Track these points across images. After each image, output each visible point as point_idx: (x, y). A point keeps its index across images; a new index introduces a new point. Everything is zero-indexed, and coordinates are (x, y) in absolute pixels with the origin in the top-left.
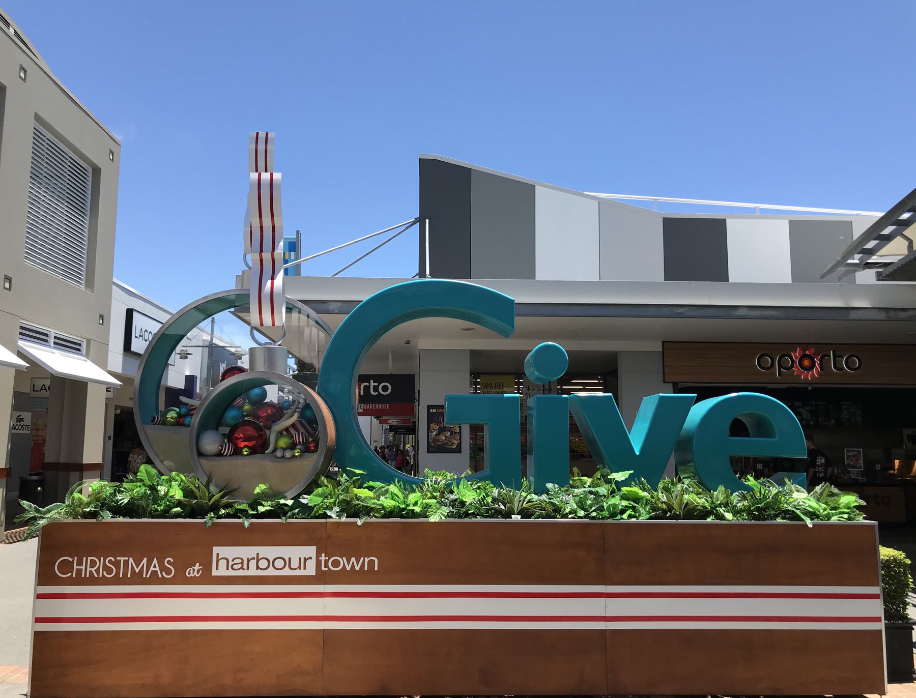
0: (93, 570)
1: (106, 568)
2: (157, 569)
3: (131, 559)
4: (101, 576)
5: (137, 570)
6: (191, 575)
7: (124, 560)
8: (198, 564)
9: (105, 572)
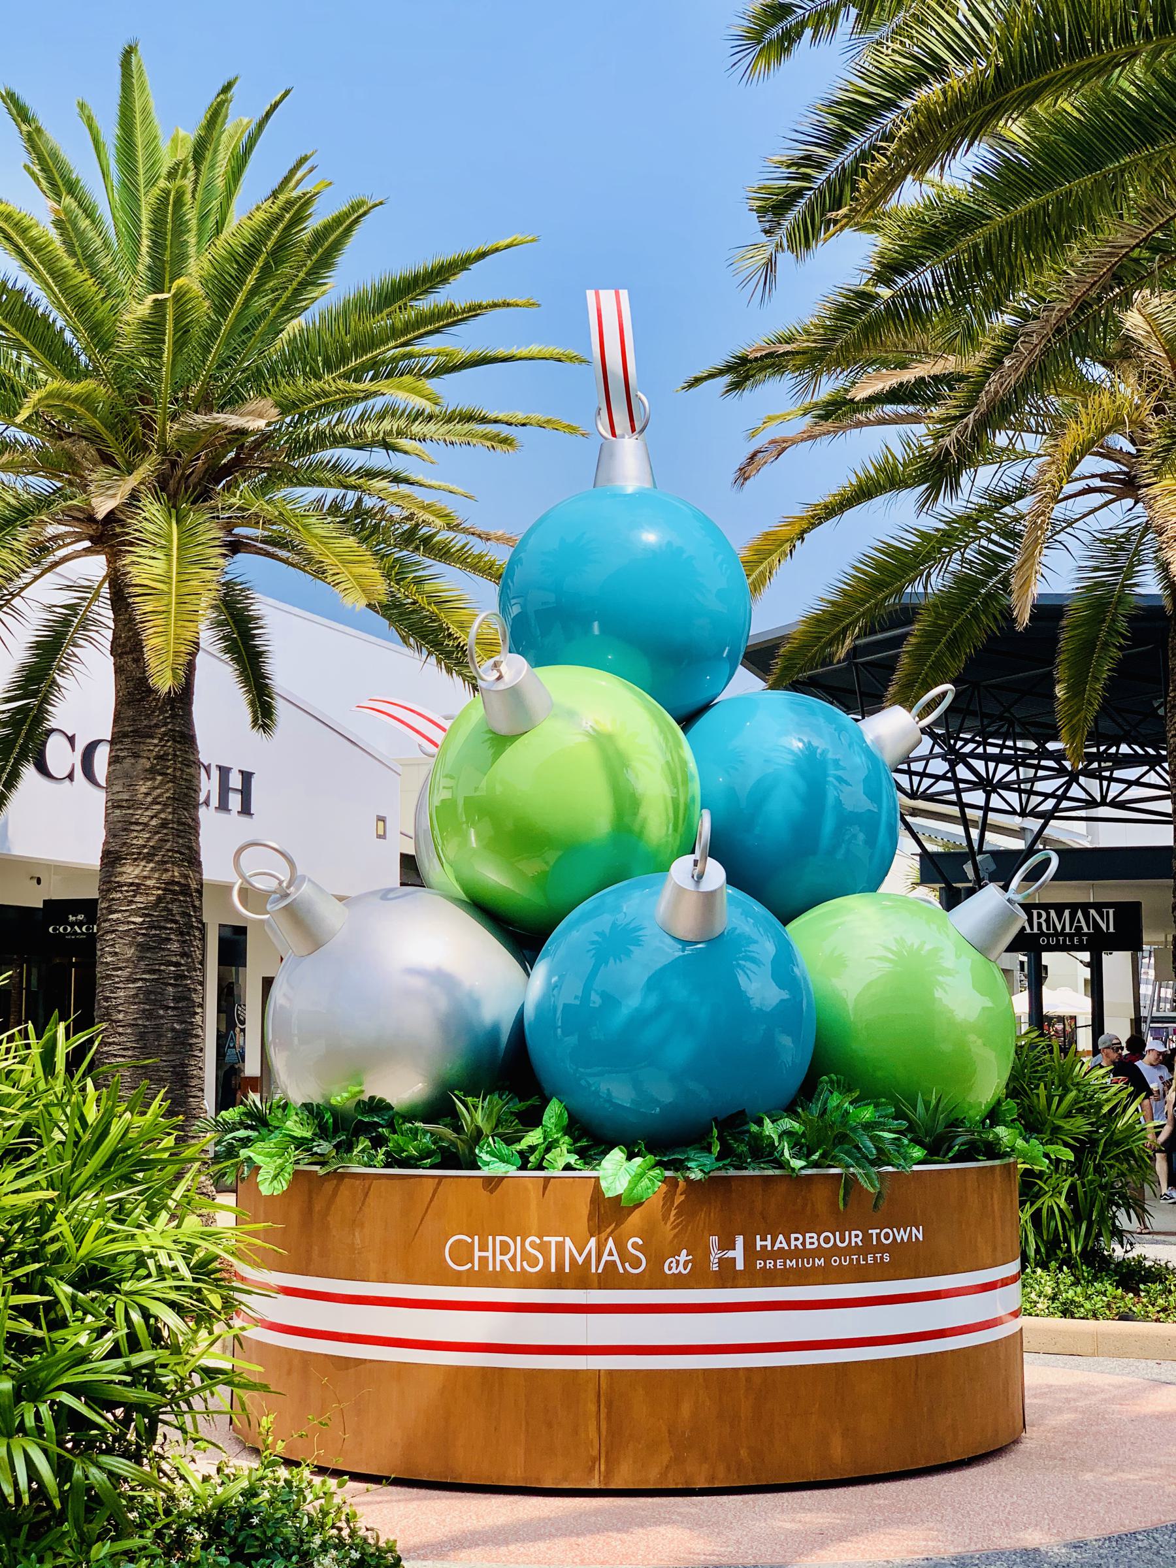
0: (506, 1258)
1: (525, 1255)
2: (616, 1258)
3: (567, 1239)
4: (518, 1269)
5: (580, 1260)
6: (674, 1271)
7: (557, 1243)
8: (684, 1252)
9: (525, 1263)
